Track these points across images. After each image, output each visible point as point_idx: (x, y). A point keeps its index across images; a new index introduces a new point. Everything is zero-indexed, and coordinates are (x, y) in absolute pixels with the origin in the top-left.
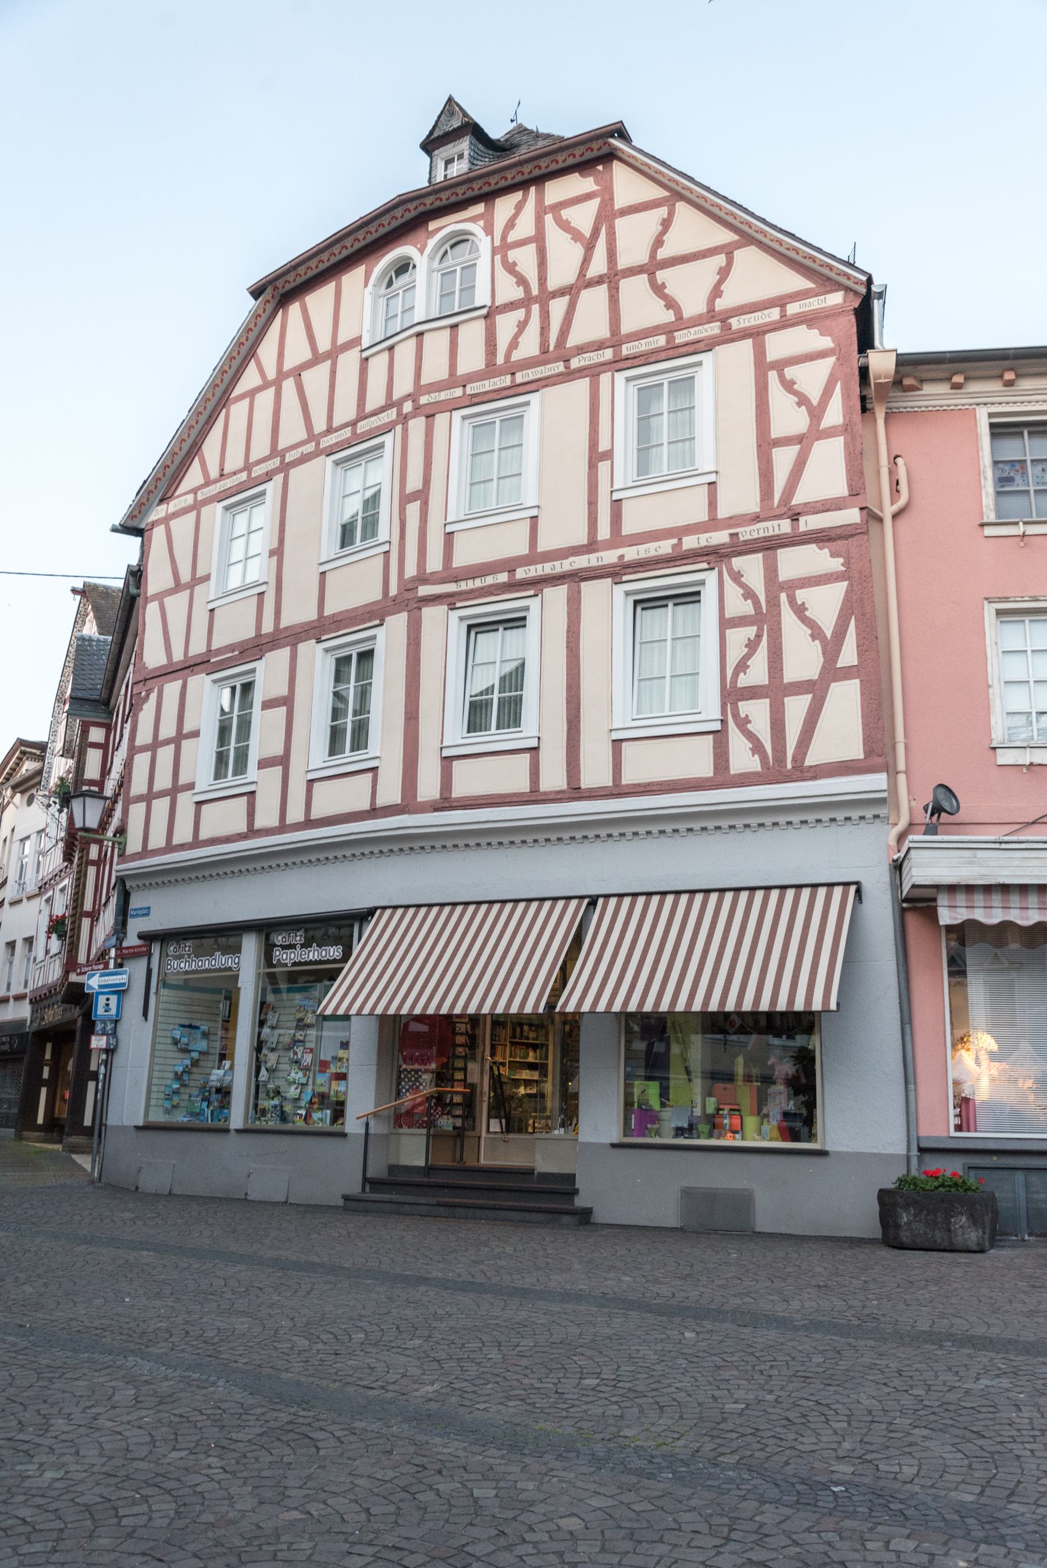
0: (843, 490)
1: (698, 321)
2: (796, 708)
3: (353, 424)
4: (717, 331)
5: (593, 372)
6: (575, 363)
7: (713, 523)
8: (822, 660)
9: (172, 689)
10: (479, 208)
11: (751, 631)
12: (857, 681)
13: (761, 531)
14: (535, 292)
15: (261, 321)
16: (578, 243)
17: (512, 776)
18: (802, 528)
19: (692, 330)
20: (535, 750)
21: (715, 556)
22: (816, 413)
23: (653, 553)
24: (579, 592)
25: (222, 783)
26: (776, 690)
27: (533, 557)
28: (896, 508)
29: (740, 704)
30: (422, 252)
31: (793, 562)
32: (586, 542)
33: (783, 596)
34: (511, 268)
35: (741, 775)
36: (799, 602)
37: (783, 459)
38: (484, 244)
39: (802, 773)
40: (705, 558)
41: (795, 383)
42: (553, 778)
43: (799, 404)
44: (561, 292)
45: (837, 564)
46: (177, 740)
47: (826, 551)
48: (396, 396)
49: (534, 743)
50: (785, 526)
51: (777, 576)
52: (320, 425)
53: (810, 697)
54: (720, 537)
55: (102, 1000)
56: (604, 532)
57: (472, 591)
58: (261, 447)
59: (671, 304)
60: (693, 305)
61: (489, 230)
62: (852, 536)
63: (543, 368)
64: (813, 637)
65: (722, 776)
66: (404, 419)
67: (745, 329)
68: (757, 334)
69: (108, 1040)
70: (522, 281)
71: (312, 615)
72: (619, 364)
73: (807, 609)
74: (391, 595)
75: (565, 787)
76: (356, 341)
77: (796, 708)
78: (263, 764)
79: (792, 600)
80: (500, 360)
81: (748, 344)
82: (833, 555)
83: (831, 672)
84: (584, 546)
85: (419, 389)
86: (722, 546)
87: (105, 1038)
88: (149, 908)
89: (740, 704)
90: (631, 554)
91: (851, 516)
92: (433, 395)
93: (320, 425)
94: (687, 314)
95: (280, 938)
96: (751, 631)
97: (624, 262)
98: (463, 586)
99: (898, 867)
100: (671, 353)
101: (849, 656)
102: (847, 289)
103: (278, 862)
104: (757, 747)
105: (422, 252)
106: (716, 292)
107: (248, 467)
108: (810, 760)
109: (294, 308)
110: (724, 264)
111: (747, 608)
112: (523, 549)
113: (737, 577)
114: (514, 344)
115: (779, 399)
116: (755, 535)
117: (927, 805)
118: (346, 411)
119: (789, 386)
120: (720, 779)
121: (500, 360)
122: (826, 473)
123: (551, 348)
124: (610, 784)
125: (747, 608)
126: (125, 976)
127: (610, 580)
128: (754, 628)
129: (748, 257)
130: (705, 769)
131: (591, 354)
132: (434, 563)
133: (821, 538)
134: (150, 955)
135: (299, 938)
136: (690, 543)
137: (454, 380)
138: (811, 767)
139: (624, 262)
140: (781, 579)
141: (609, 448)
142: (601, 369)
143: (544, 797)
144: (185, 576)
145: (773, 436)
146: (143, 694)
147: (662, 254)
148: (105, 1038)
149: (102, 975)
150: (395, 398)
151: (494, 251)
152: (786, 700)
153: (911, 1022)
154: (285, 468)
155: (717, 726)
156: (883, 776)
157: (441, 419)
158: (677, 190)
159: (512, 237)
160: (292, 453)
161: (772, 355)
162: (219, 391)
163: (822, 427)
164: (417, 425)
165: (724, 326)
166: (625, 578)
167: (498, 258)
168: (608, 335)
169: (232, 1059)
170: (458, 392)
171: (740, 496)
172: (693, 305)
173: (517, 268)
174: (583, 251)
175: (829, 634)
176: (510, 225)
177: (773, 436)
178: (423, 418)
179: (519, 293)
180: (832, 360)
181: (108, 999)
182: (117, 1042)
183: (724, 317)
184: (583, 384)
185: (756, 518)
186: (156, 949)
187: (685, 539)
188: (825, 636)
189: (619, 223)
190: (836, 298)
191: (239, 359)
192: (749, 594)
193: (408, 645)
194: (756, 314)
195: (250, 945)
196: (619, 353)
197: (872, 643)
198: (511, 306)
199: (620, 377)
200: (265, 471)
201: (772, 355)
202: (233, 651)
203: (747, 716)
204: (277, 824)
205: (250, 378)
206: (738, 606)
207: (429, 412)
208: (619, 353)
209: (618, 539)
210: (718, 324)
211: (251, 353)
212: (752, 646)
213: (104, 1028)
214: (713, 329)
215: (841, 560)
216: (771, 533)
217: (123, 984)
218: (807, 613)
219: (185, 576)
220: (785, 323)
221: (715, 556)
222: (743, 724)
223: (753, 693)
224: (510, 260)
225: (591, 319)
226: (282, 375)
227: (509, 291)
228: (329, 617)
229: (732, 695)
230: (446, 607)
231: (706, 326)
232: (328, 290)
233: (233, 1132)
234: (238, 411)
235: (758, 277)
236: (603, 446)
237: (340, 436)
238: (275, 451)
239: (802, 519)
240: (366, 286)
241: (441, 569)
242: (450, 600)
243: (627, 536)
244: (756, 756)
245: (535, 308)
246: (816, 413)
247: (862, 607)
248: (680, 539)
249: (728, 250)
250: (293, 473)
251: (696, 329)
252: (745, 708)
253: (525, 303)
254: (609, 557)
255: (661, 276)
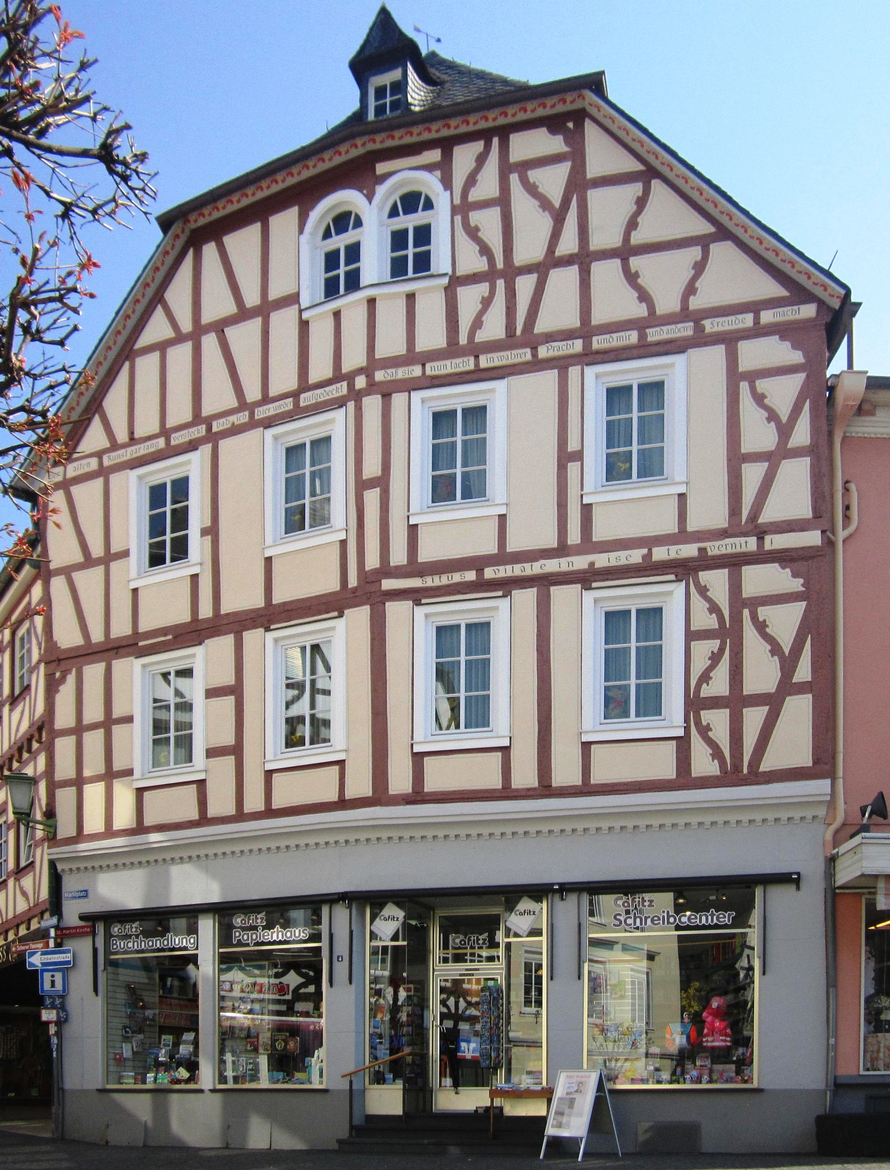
0: (806, 512)
1: (670, 319)
2: (754, 718)
3: (295, 395)
4: (690, 333)
5: (562, 364)
6: (543, 352)
7: (682, 536)
8: (780, 674)
9: (94, 672)
10: (434, 155)
11: (715, 644)
12: (810, 696)
13: (729, 547)
14: (500, 265)
15: (170, 260)
16: (547, 213)
17: (486, 773)
18: (768, 546)
19: (665, 328)
20: (505, 750)
21: (683, 570)
22: (785, 431)
23: (623, 562)
24: (549, 596)
25: (162, 771)
26: (736, 701)
27: (502, 557)
28: (847, 532)
29: (702, 713)
30: (370, 198)
31: (760, 579)
32: (555, 545)
33: (746, 612)
34: (473, 233)
35: (701, 778)
36: (761, 619)
37: (752, 475)
38: (443, 201)
39: (757, 777)
40: (674, 570)
41: (766, 397)
42: (525, 775)
43: (769, 420)
44: (528, 269)
45: (797, 585)
46: (108, 723)
47: (788, 570)
48: (346, 368)
49: (506, 743)
50: (750, 544)
51: (741, 592)
52: (253, 393)
53: (767, 708)
54: (689, 551)
55: (47, 976)
56: (574, 537)
57: (438, 588)
58: (180, 411)
59: (644, 296)
60: (667, 301)
61: (447, 183)
62: (812, 557)
63: (508, 353)
64: (773, 652)
65: (684, 779)
66: (356, 396)
67: (718, 334)
68: (730, 340)
69: (58, 1014)
70: (485, 250)
71: (259, 602)
72: (590, 357)
73: (767, 626)
74: (350, 586)
75: (536, 784)
76: (293, 299)
77: (754, 718)
78: (211, 753)
79: (754, 617)
80: (463, 340)
81: (719, 351)
82: (795, 575)
83: (788, 686)
84: (553, 549)
85: (372, 364)
86: (692, 559)
87: (54, 1012)
88: (86, 891)
89: (702, 713)
90: (602, 560)
91: (813, 538)
92: (389, 371)
93: (253, 393)
94: (660, 310)
95: (239, 920)
96: (715, 644)
97: (597, 242)
98: (430, 582)
99: (832, 861)
100: (642, 351)
101: (803, 672)
102: (821, 303)
103: (234, 849)
104: (717, 753)
105: (370, 198)
106: (690, 290)
107: (165, 432)
108: (766, 765)
109: (210, 250)
110: (699, 258)
111: (712, 622)
112: (492, 548)
113: (703, 591)
114: (477, 324)
115: (751, 416)
116: (724, 551)
117: (866, 807)
118: (284, 379)
119: (759, 399)
120: (682, 781)
121: (463, 340)
122: (791, 493)
123: (519, 332)
124: (580, 783)
125: (712, 622)
126: (69, 955)
127: (579, 586)
128: (718, 642)
129: (723, 253)
130: (668, 771)
131: (560, 344)
132: (399, 556)
133: (783, 557)
134: (94, 934)
135: (260, 919)
136: (660, 554)
137: (411, 357)
138: (765, 772)
139: (597, 242)
140: (744, 596)
141: (579, 448)
142: (569, 360)
143: (515, 794)
144: (97, 551)
145: (743, 451)
146: (58, 675)
147: (637, 238)
148: (54, 1012)
149: (43, 954)
150: (345, 370)
151: (454, 210)
152: (745, 710)
153: (835, 986)
154: (213, 438)
155: (680, 732)
156: (828, 782)
157: (398, 400)
158: (654, 166)
159: (475, 195)
160: (221, 421)
161: (744, 365)
162: (121, 339)
163: (790, 446)
164: (372, 404)
165: (695, 328)
166: (594, 585)
167: (458, 219)
168: (578, 324)
169: (196, 1031)
170: (417, 371)
171: (710, 512)
172: (667, 301)
173: (480, 234)
174: (552, 223)
175: (787, 651)
176: (471, 181)
177: (743, 451)
178: (379, 397)
179: (482, 265)
180: (800, 377)
181: (53, 976)
182: (67, 1015)
183: (697, 318)
184: (551, 377)
185: (723, 534)
186: (100, 928)
187: (655, 550)
188: (783, 653)
189: (594, 196)
190: (808, 311)
191: (144, 302)
192: (714, 608)
193: (373, 639)
194: (730, 318)
195: (207, 926)
196: (590, 343)
197: (825, 661)
198: (473, 279)
199: (590, 372)
200: (187, 439)
201: (744, 365)
202: (166, 635)
203: (708, 724)
204: (234, 813)
205: (157, 329)
206: (704, 620)
207: (385, 391)
208: (590, 343)
209: (588, 545)
210: (692, 324)
211: (158, 299)
212: (715, 658)
213: (53, 1002)
214: (686, 330)
215: (801, 581)
216: (738, 550)
217: (68, 962)
218: (767, 630)
219: (97, 551)
220: (758, 331)
221: (683, 570)
222: (704, 731)
223: (715, 703)
224: (472, 224)
225: (559, 307)
226: (199, 330)
227: (471, 261)
228: (279, 605)
229: (694, 704)
230: (411, 603)
231: (680, 326)
232: (251, 233)
233: (207, 1092)
234: (147, 367)
235: (732, 279)
236: (573, 445)
237: (279, 407)
238: (197, 418)
239: (768, 539)
240: (301, 231)
241: (405, 562)
242: (416, 595)
243: (598, 542)
244: (716, 761)
245: (500, 284)
246: (785, 431)
247: (818, 628)
248: (650, 550)
249: (704, 242)
250: (223, 444)
251: (669, 327)
252: (707, 716)
253: (489, 276)
254: (580, 563)
255: (635, 262)
